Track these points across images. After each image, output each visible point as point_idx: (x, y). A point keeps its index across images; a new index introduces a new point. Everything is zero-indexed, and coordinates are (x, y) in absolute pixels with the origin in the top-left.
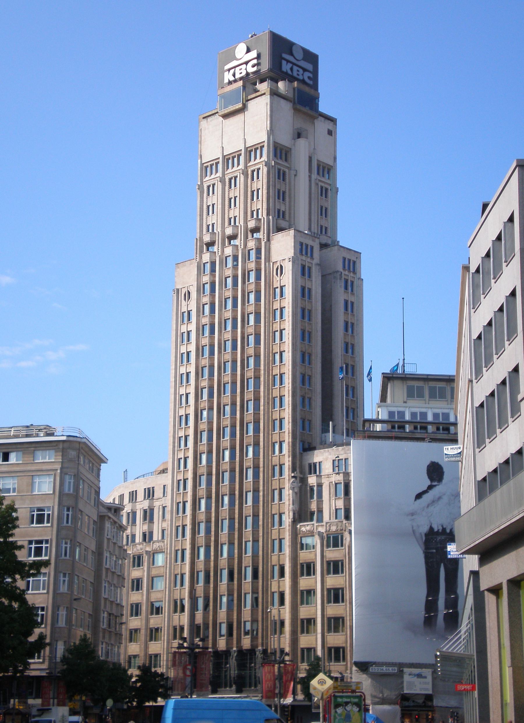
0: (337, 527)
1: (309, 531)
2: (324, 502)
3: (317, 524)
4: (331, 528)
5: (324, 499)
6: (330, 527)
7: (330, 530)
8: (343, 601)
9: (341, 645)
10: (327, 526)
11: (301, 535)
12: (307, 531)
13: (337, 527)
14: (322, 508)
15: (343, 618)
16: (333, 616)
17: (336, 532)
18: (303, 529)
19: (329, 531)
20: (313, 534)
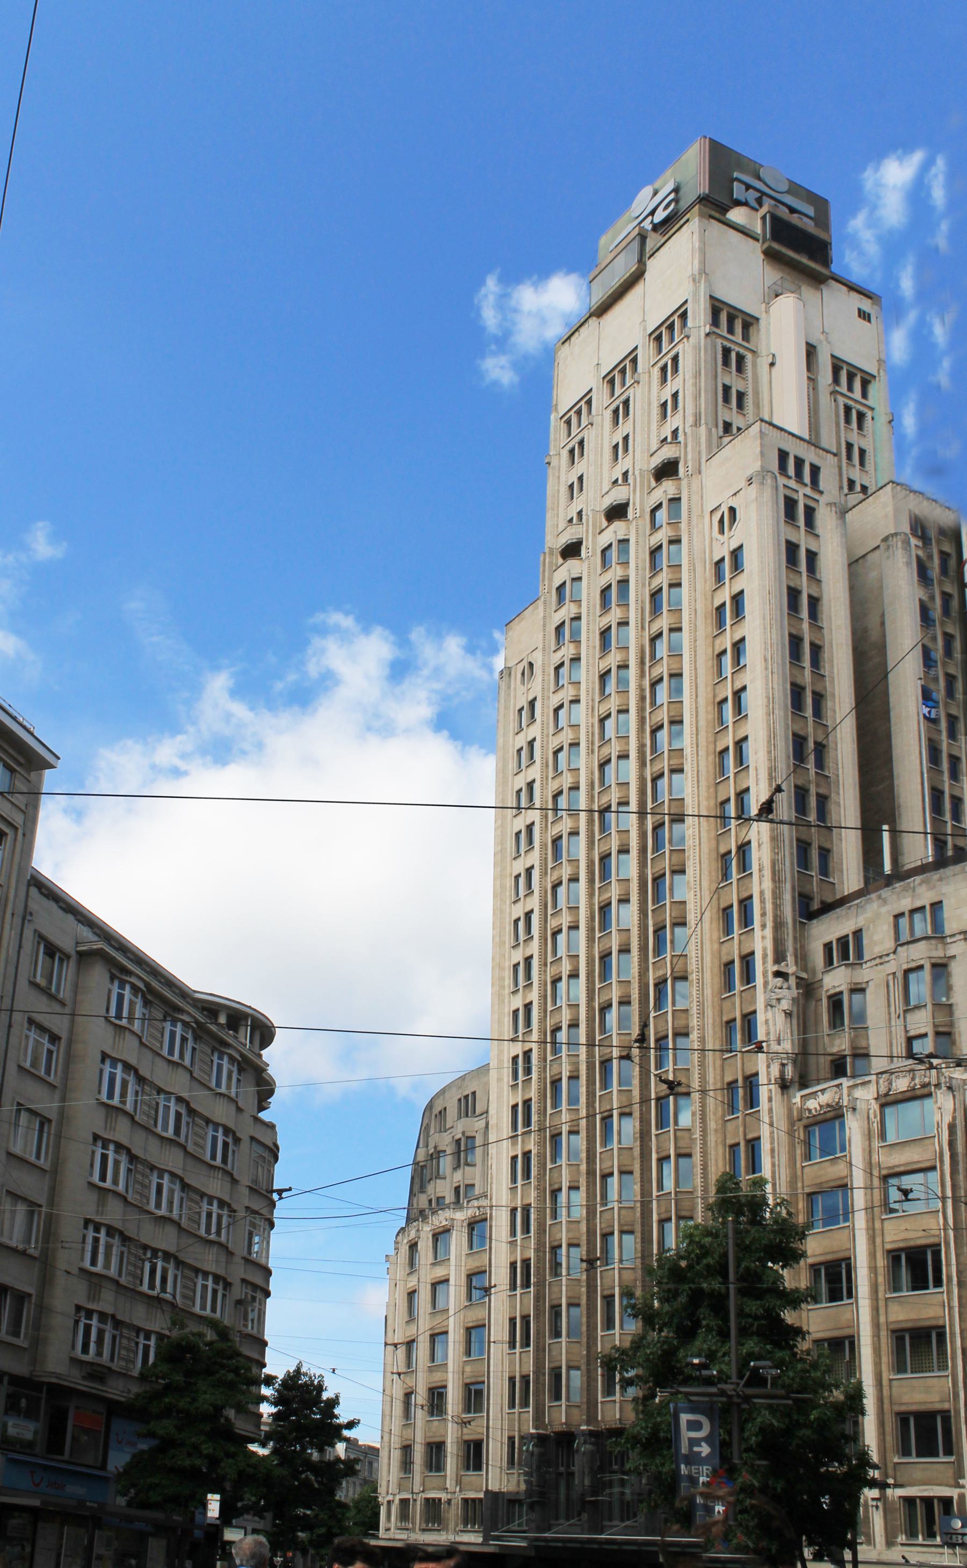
0: (913, 1079)
1: (828, 1105)
2: (870, 1032)
3: (851, 1083)
4: (894, 1084)
5: (870, 1023)
6: (891, 1084)
7: (890, 1090)
8: (938, 1282)
9: (938, 1406)
10: (881, 1081)
11: (805, 1122)
12: (821, 1106)
13: (913, 1079)
14: (867, 1048)
15: (941, 1336)
16: (909, 1325)
17: (908, 1094)
18: (812, 1104)
19: (887, 1095)
20: (840, 1112)
